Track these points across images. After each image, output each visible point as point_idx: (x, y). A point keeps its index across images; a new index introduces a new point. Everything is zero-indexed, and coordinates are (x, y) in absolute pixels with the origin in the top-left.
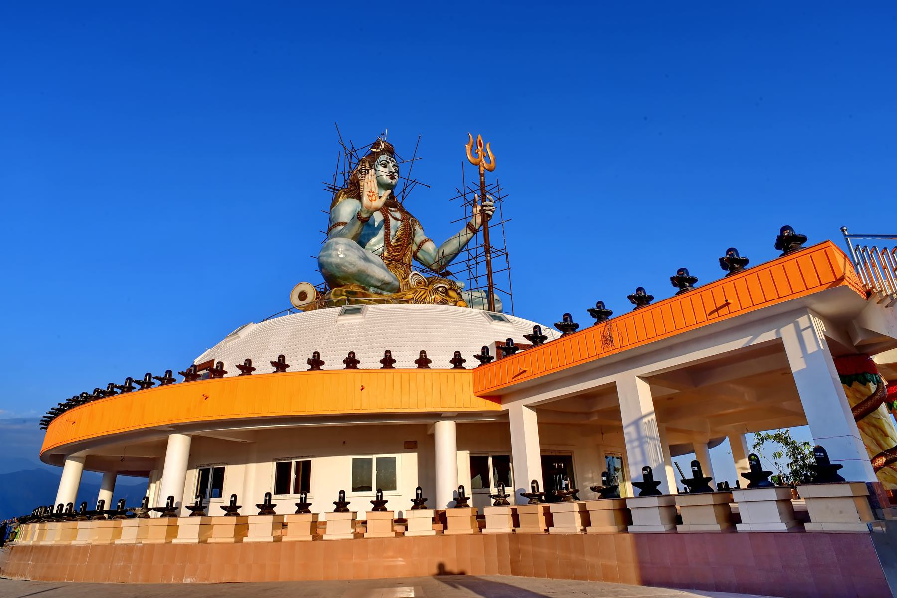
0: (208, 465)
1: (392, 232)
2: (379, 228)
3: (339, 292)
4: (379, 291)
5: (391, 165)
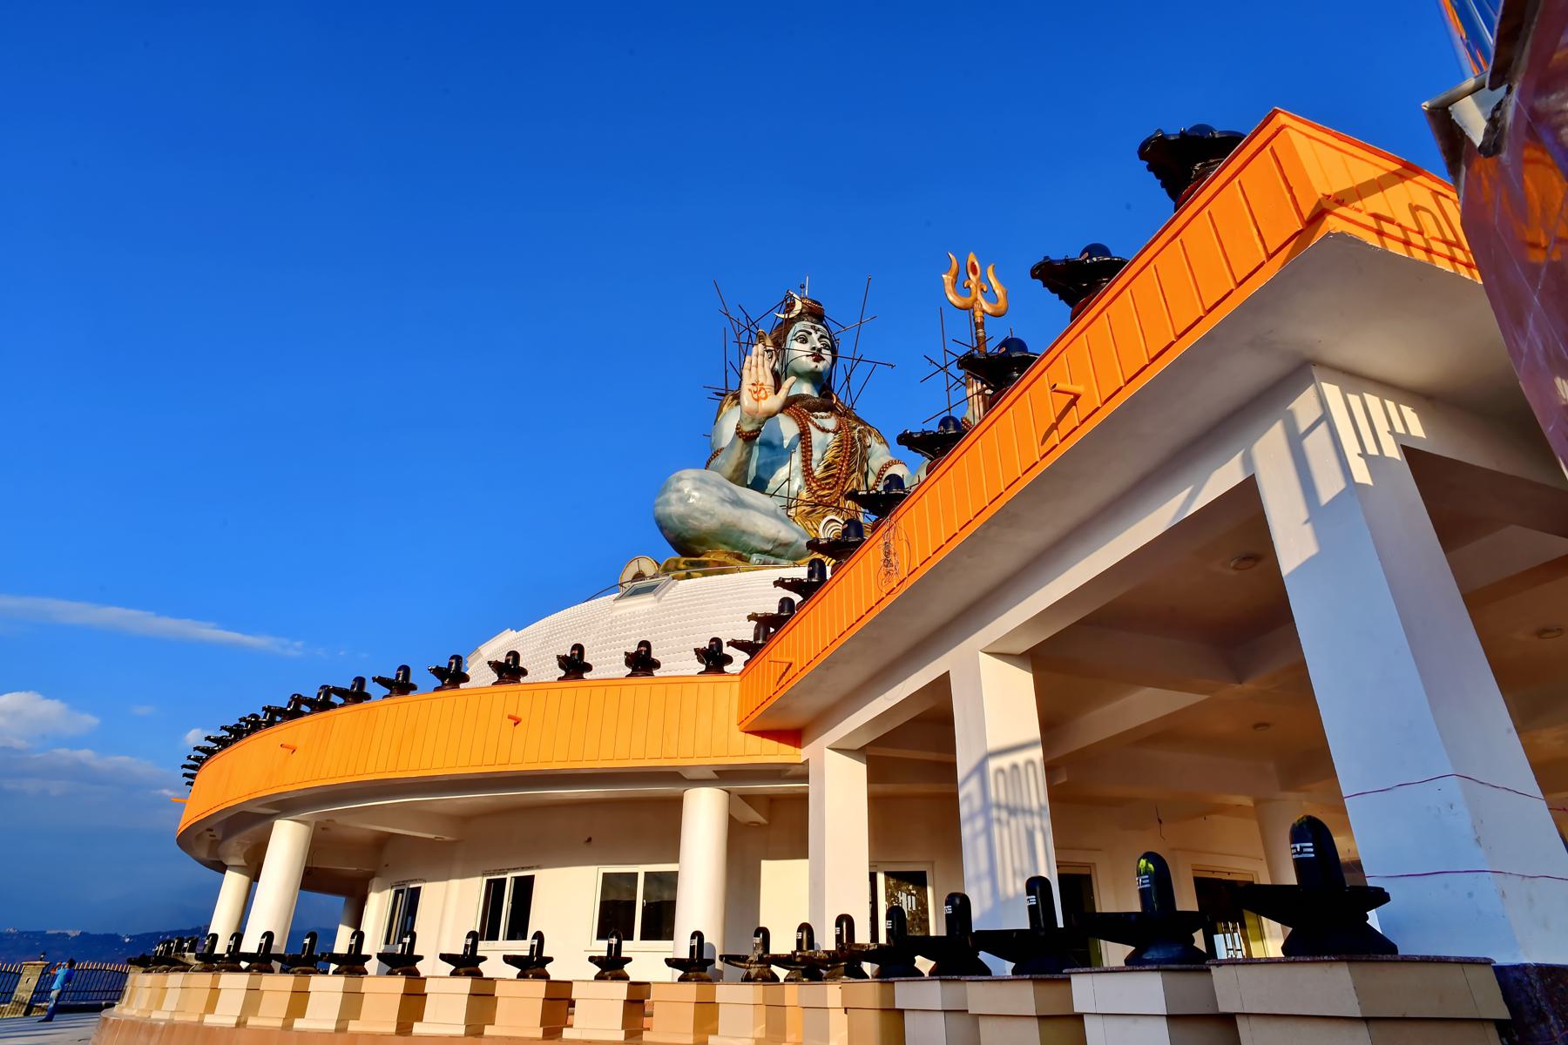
0: (404, 883)
1: (817, 455)
2: (792, 447)
3: (672, 565)
4: (772, 559)
5: (815, 336)
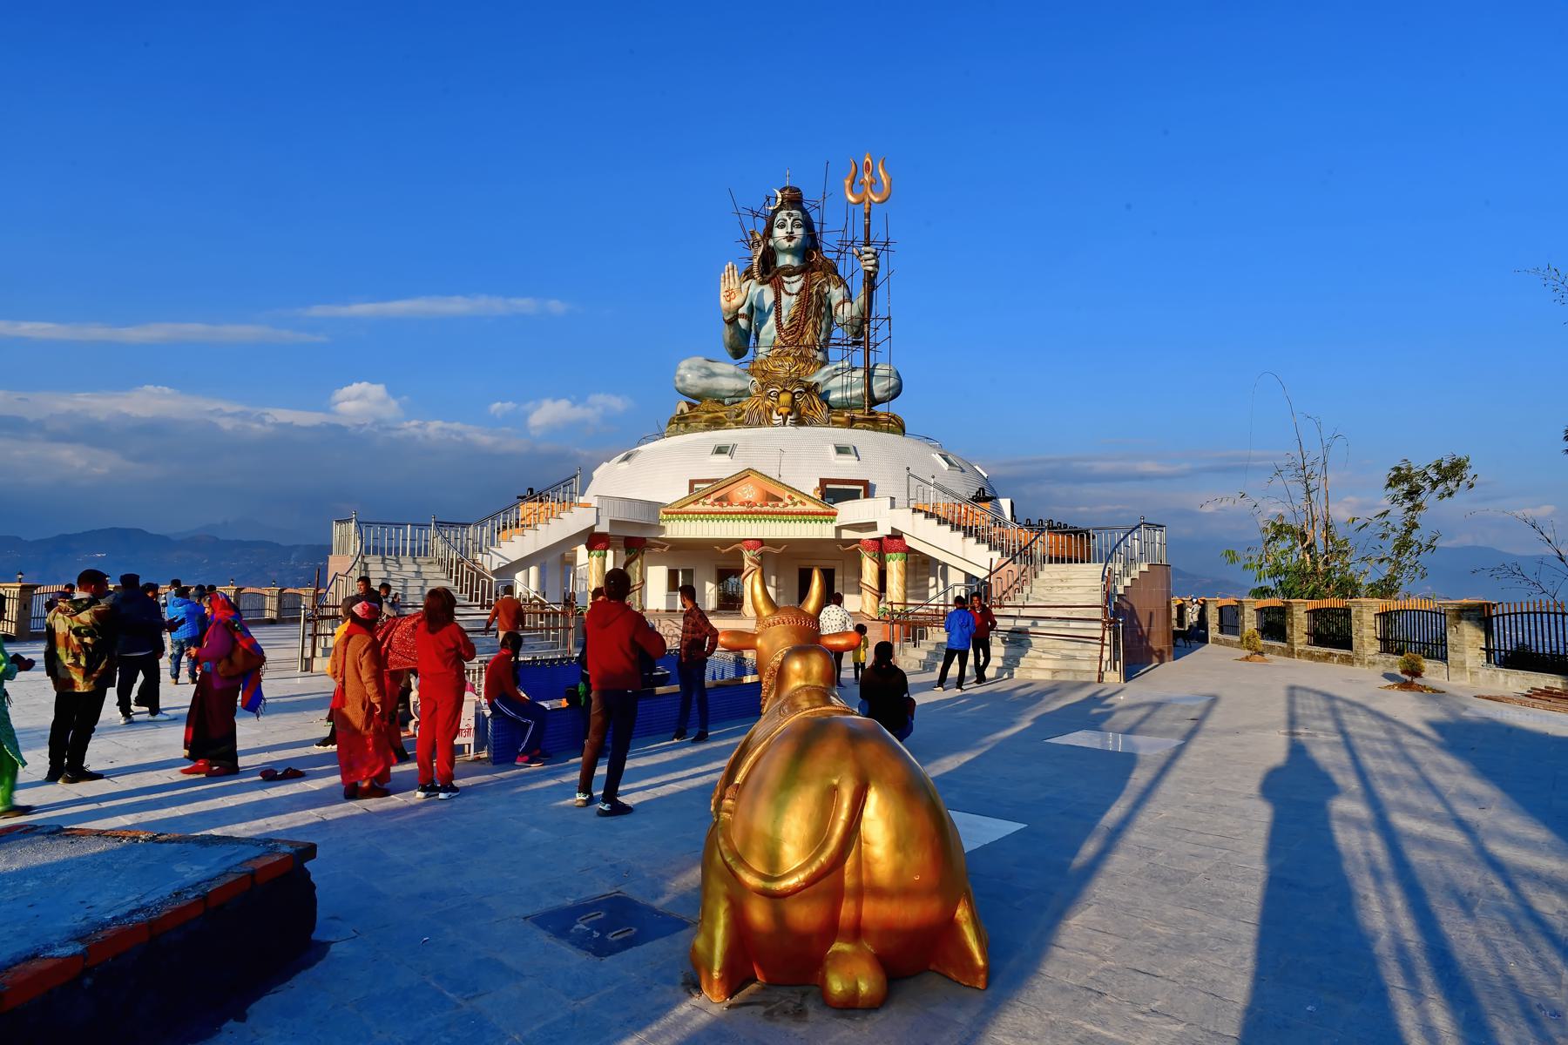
1: (784, 313)
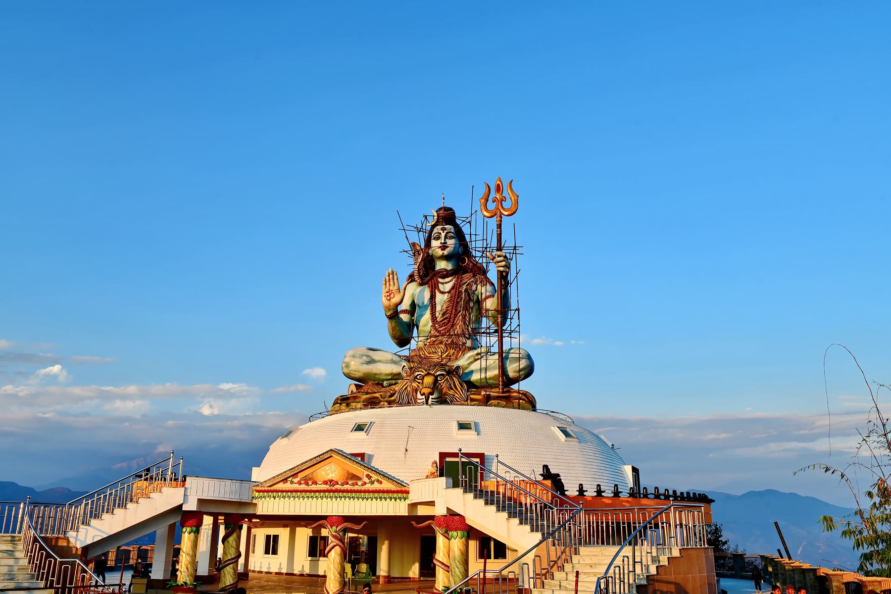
1: (438, 308)
2: (426, 306)
4: (394, 382)
5: (443, 235)
